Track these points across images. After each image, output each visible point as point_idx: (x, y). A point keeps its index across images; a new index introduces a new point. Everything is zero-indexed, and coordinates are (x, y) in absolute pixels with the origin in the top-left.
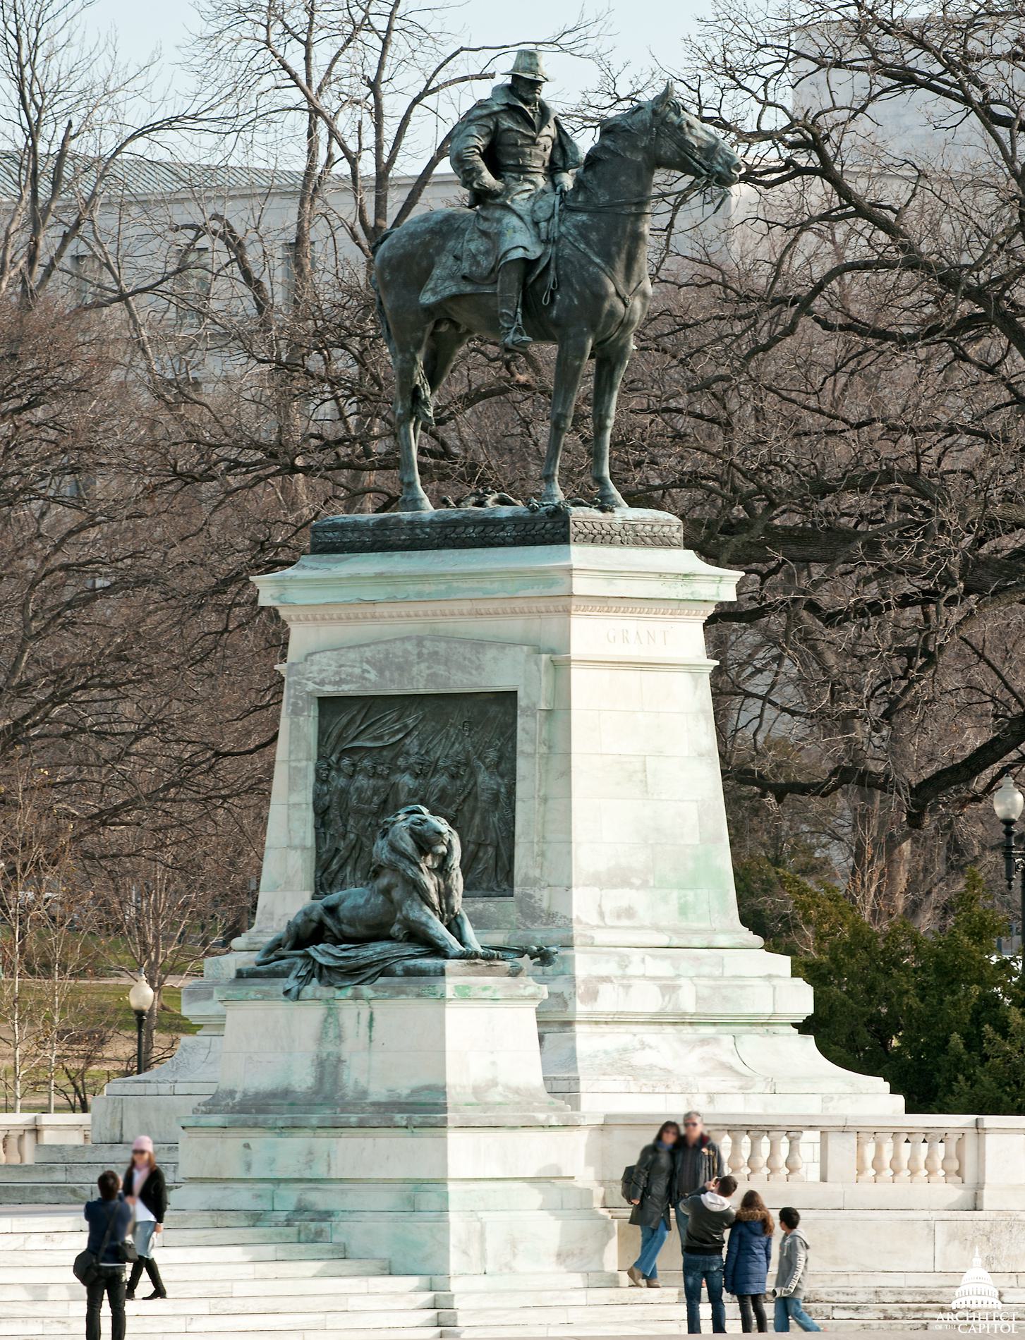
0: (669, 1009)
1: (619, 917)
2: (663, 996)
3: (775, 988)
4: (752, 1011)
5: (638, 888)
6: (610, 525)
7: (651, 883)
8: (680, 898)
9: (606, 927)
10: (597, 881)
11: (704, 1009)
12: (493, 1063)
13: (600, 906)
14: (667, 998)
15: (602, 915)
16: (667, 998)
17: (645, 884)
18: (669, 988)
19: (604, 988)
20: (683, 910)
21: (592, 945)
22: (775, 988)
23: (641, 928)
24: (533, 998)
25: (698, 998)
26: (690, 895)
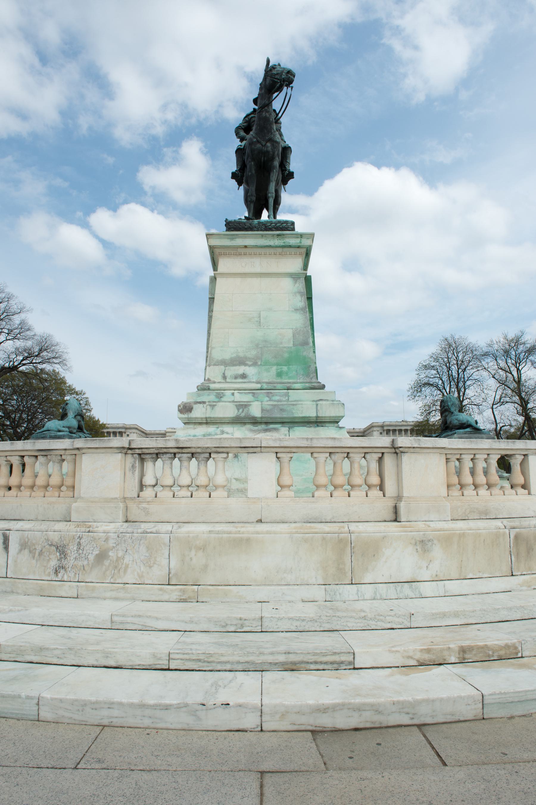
0: (243, 415)
1: (236, 378)
2: (238, 410)
5: (250, 366)
6: (250, 224)
7: (259, 363)
8: (277, 370)
10: (224, 363)
11: (267, 415)
13: (224, 374)
14: (241, 410)
15: (224, 377)
16: (241, 410)
17: (255, 364)
19: (195, 406)
20: (279, 374)
21: (209, 389)
22: (317, 405)
25: (263, 410)
26: (285, 368)
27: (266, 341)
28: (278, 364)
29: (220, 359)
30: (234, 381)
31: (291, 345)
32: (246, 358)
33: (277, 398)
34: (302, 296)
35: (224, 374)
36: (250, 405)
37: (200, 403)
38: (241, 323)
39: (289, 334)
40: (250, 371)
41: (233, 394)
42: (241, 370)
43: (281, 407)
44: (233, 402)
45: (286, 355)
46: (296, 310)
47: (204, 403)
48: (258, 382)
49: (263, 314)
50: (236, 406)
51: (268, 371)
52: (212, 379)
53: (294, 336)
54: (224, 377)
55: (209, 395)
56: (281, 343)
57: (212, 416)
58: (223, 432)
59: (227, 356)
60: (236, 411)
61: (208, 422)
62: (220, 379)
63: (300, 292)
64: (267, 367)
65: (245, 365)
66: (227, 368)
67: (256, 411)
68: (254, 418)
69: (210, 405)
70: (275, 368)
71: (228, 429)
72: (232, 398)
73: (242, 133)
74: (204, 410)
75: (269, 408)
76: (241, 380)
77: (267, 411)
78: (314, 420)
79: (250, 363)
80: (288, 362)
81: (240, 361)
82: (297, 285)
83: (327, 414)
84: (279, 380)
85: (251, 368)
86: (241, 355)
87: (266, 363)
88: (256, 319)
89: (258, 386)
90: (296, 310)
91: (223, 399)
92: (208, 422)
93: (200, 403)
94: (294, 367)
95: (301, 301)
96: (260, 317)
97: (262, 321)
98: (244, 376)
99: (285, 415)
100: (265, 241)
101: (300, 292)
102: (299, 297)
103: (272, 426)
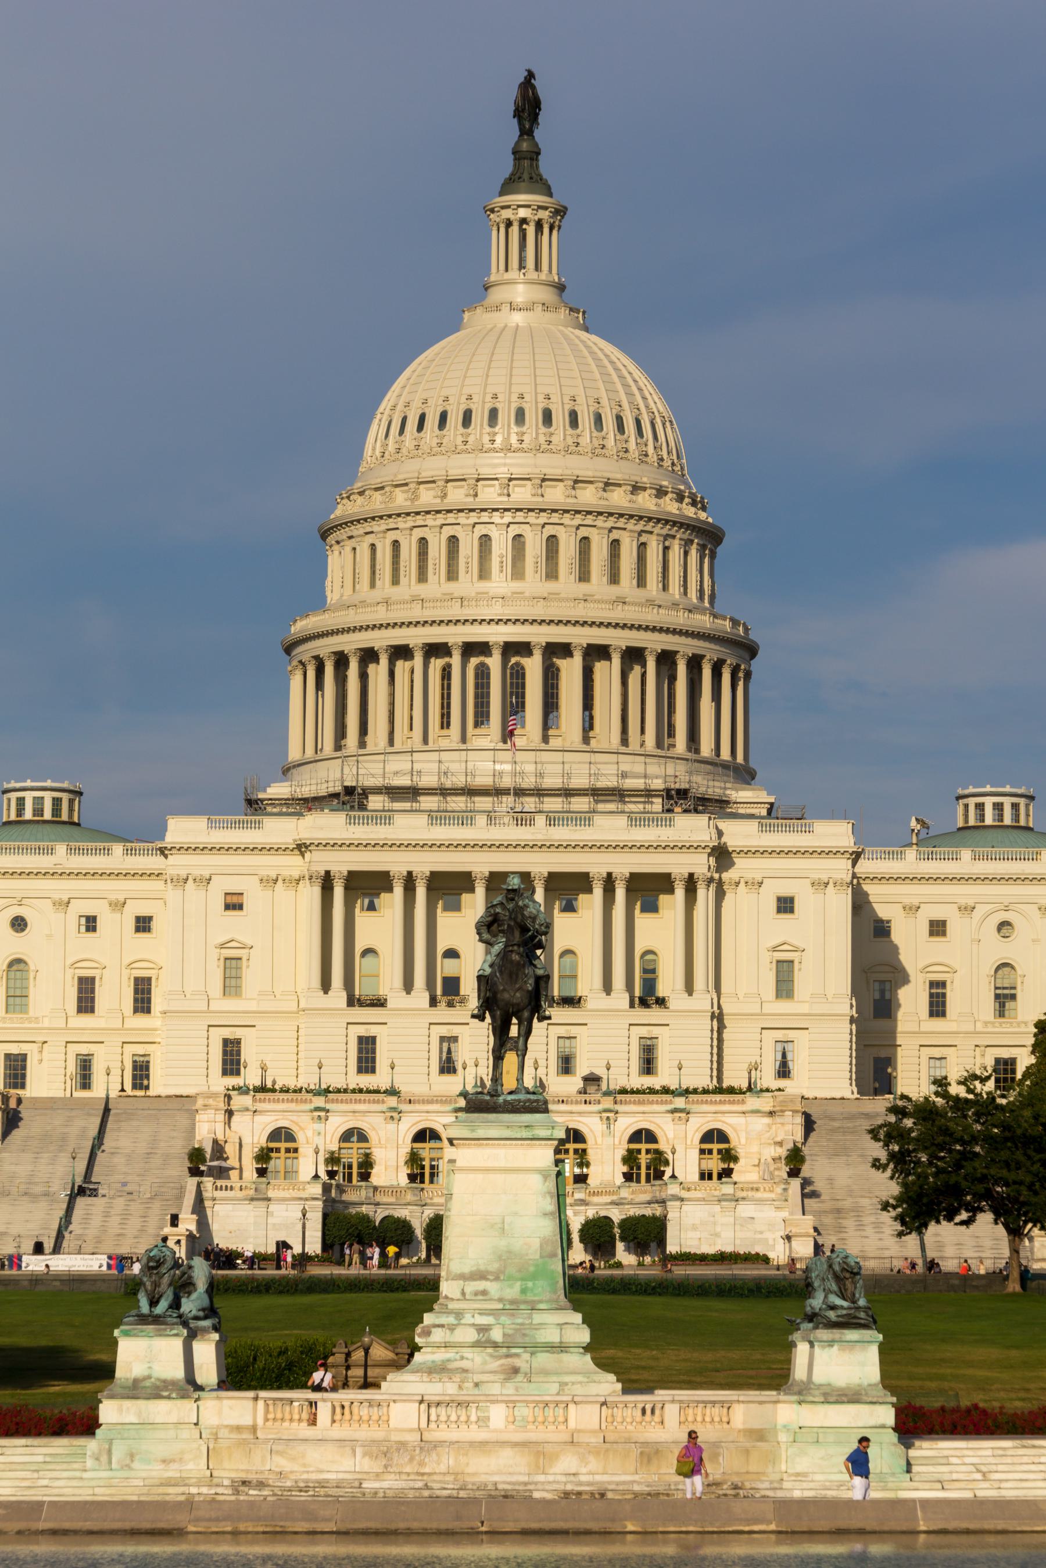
2: (479, 1334)
3: (561, 1329)
4: (543, 1341)
5: (491, 1281)
7: (502, 1278)
8: (521, 1285)
9: (465, 1299)
10: (463, 1277)
11: (509, 1340)
12: (150, 1368)
13: (463, 1290)
14: (481, 1335)
15: (463, 1293)
16: (481, 1335)
17: (497, 1279)
18: (483, 1329)
19: (434, 1330)
20: (524, 1291)
23: (491, 1300)
24: (176, 1335)
25: (504, 1335)
26: (530, 1284)
27: (509, 1252)
28: (522, 1279)
29: (459, 1272)
30: (473, 1298)
31: (537, 1256)
32: (488, 1272)
33: (520, 1321)
34: (552, 1197)
35: (463, 1290)
36: (491, 1329)
37: (439, 1326)
38: (483, 1230)
39: (536, 1243)
40: (493, 1288)
41: (473, 1316)
42: (481, 1285)
43: (524, 1332)
44: (474, 1325)
45: (532, 1269)
46: (545, 1214)
47: (442, 1326)
48: (500, 1300)
49: (507, 1220)
50: (477, 1330)
51: (511, 1287)
52: (450, 1296)
53: (541, 1246)
54: (463, 1293)
55: (447, 1317)
56: (527, 1255)
57: (451, 1340)
58: (462, 1358)
59: (466, 1270)
60: (477, 1336)
61: (446, 1346)
62: (458, 1296)
63: (549, 1193)
64: (510, 1282)
65: (487, 1279)
66: (466, 1283)
67: (497, 1335)
68: (495, 1342)
69: (449, 1329)
70: (519, 1283)
71: (468, 1353)
72: (471, 1321)
73: (484, 930)
74: (443, 1334)
75: (510, 1332)
76: (481, 1297)
77: (509, 1335)
78: (559, 1345)
79: (491, 1277)
80: (534, 1277)
81: (480, 1275)
82: (547, 1184)
83: (572, 1340)
84: (523, 1297)
85: (494, 1283)
86: (482, 1268)
87: (510, 1278)
88: (499, 1226)
89: (500, 1306)
90: (545, 1214)
91: (462, 1322)
92: (446, 1346)
93: (439, 1326)
94: (540, 1283)
95: (551, 1204)
96: (503, 1223)
97: (506, 1227)
98: (484, 1293)
99: (527, 1339)
100: (512, 1133)
101: (549, 1193)
102: (548, 1199)
103: (514, 1351)
